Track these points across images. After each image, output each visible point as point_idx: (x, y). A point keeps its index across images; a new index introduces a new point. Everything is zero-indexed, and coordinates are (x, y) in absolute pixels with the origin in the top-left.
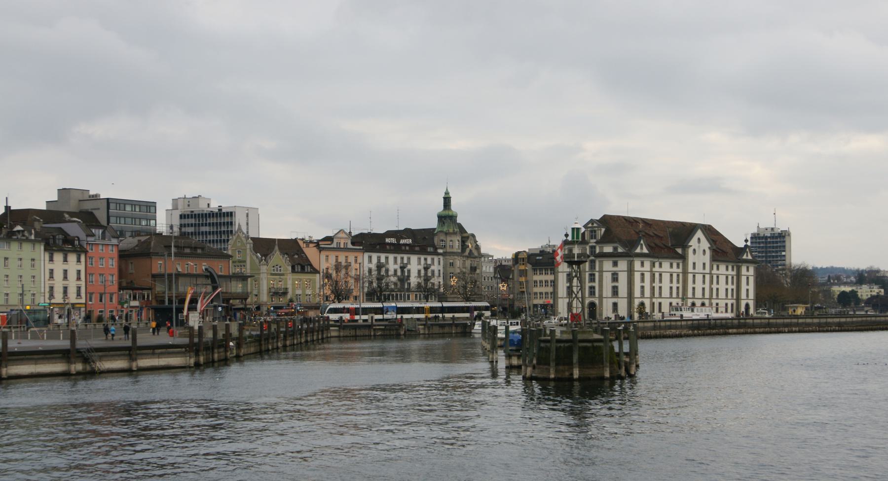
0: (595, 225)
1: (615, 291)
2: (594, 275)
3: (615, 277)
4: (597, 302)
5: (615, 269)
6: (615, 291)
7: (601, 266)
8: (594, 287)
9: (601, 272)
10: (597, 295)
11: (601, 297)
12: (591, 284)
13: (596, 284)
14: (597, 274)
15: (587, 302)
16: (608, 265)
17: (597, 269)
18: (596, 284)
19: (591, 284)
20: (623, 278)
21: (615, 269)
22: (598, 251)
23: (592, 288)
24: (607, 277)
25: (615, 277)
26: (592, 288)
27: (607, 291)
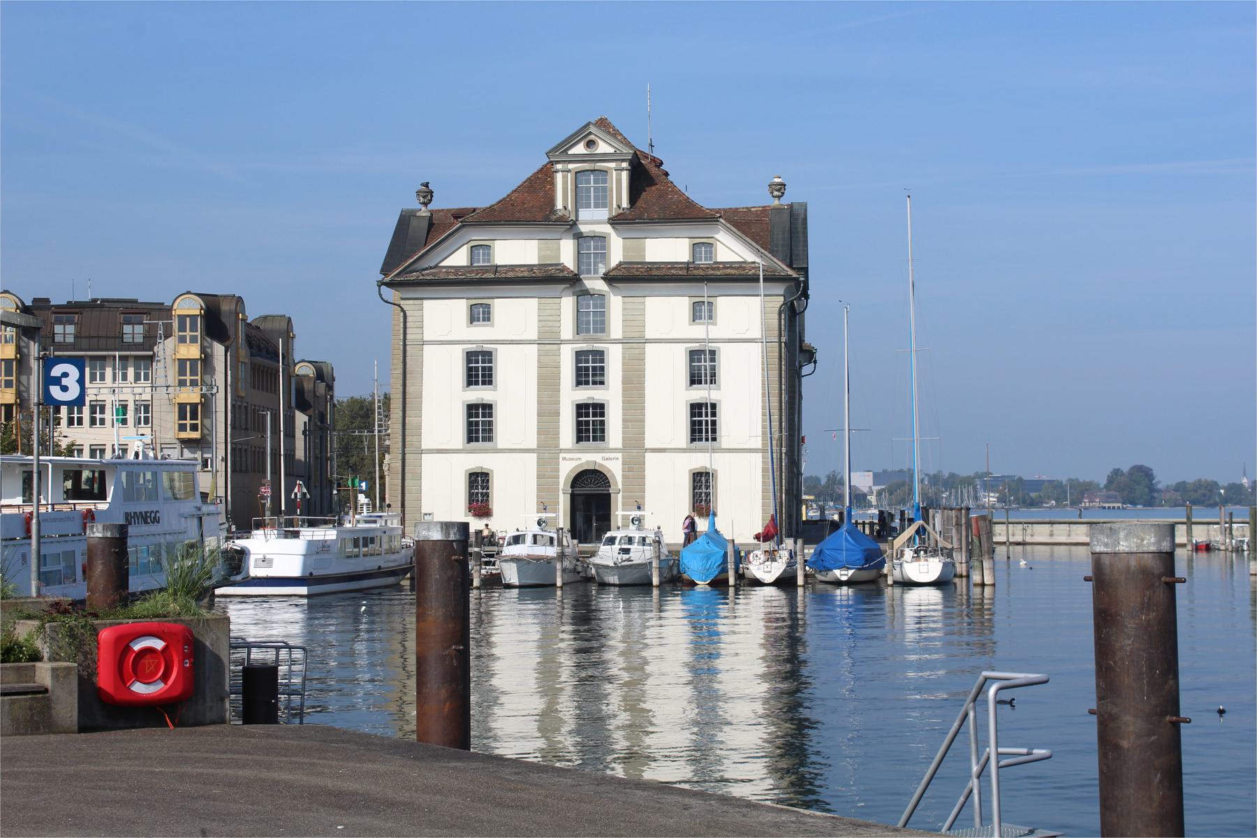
0: (603, 148)
4: (614, 467)
8: (599, 409)
9: (635, 342)
11: (635, 447)
15: (568, 467)
16: (667, 312)
18: (611, 395)
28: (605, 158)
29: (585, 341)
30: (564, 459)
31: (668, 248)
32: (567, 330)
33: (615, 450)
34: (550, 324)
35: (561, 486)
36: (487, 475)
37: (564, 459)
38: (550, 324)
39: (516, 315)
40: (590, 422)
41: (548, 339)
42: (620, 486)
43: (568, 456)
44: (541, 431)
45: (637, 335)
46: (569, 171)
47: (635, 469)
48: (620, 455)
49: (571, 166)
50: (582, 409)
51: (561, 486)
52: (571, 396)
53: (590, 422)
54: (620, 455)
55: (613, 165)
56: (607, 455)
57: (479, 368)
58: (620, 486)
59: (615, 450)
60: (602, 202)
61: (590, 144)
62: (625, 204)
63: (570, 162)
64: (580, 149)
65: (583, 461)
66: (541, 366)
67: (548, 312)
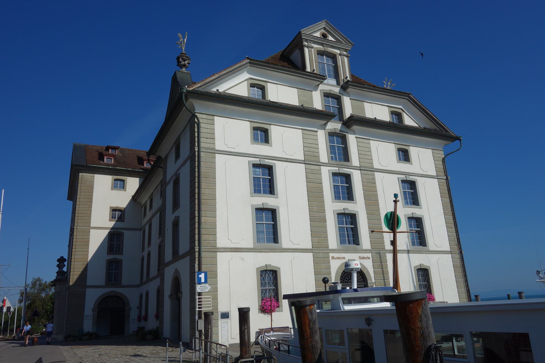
7: (365, 154)
8: (352, 218)
14: (357, 178)
16: (384, 152)
17: (355, 159)
30: (333, 258)
33: (366, 251)
37: (333, 258)
38: (312, 150)
39: (287, 139)
41: (310, 161)
43: (336, 255)
46: (312, 48)
48: (370, 255)
52: (332, 207)
54: (370, 255)
55: (338, 52)
57: (265, 178)
58: (374, 281)
59: (366, 251)
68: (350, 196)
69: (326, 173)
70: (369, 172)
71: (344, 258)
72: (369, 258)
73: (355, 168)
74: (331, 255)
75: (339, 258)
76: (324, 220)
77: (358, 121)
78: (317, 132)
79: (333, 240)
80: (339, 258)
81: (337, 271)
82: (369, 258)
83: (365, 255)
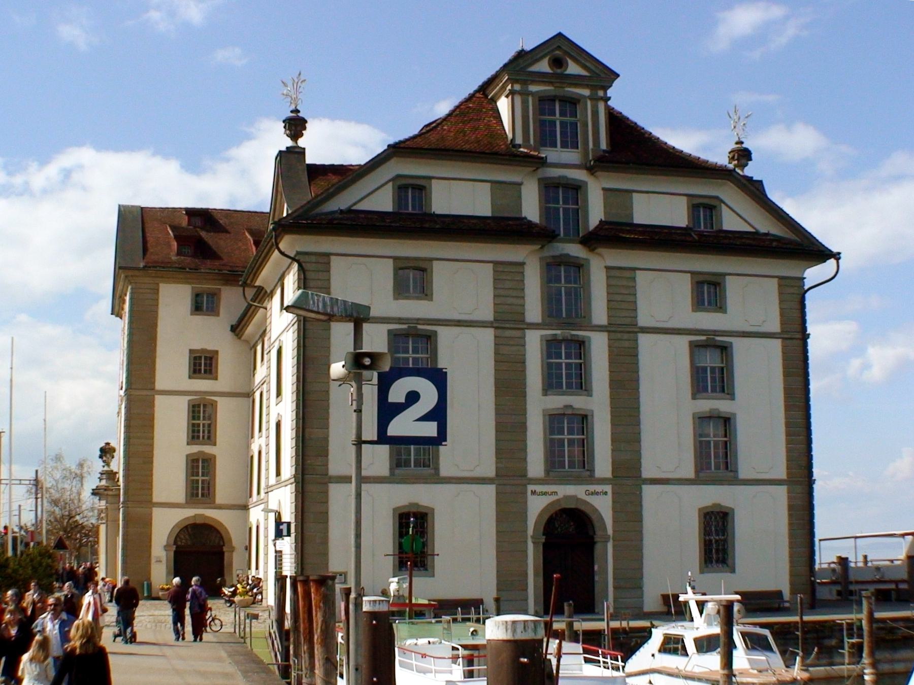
0: (573, 69)
1: (716, 452)
2: (581, 346)
3: (713, 369)
4: (602, 504)
5: (709, 321)
6: (716, 452)
9: (625, 332)
10: (603, 465)
11: (628, 476)
12: (557, 402)
13: (598, 403)
14: (599, 347)
15: (537, 506)
16: (663, 292)
19: (557, 402)
20: (757, 367)
21: (709, 321)
22: (596, 213)
23: (571, 428)
24: (664, 368)
25: (713, 369)
26: (571, 428)
27: (667, 443)
28: (576, 80)
29: (560, 326)
30: (534, 493)
31: (660, 205)
32: (534, 310)
33: (602, 481)
34: (510, 300)
35: (530, 532)
36: (426, 514)
37: (534, 493)
38: (510, 300)
39: (463, 284)
40: (569, 439)
41: (507, 322)
42: (610, 531)
43: (539, 488)
44: (500, 453)
45: (628, 321)
46: (532, 94)
47: (630, 510)
48: (608, 488)
49: (533, 88)
50: (554, 421)
51: (530, 532)
53: (569, 439)
54: (608, 488)
55: (586, 92)
56: (592, 488)
58: (610, 531)
59: (602, 481)
60: (570, 141)
61: (558, 63)
62: (604, 145)
63: (533, 82)
64: (543, 66)
65: (560, 496)
66: (500, 359)
67: (508, 284)
68: (580, 382)
69: (534, 342)
70: (626, 336)
71: (556, 493)
72: (606, 493)
73: (600, 328)
74: (531, 488)
75: (545, 494)
76: (522, 427)
77: (619, 234)
78: (522, 264)
79: (536, 464)
80: (545, 494)
81: (540, 515)
82: (606, 493)
83: (598, 488)
